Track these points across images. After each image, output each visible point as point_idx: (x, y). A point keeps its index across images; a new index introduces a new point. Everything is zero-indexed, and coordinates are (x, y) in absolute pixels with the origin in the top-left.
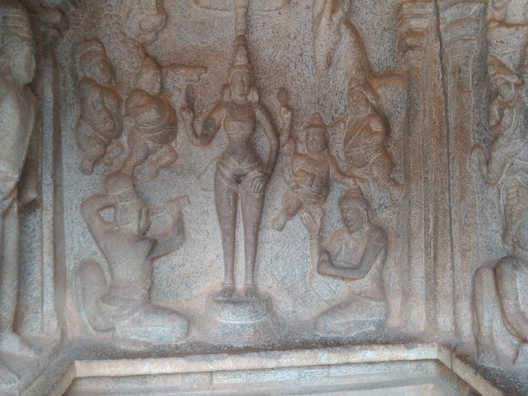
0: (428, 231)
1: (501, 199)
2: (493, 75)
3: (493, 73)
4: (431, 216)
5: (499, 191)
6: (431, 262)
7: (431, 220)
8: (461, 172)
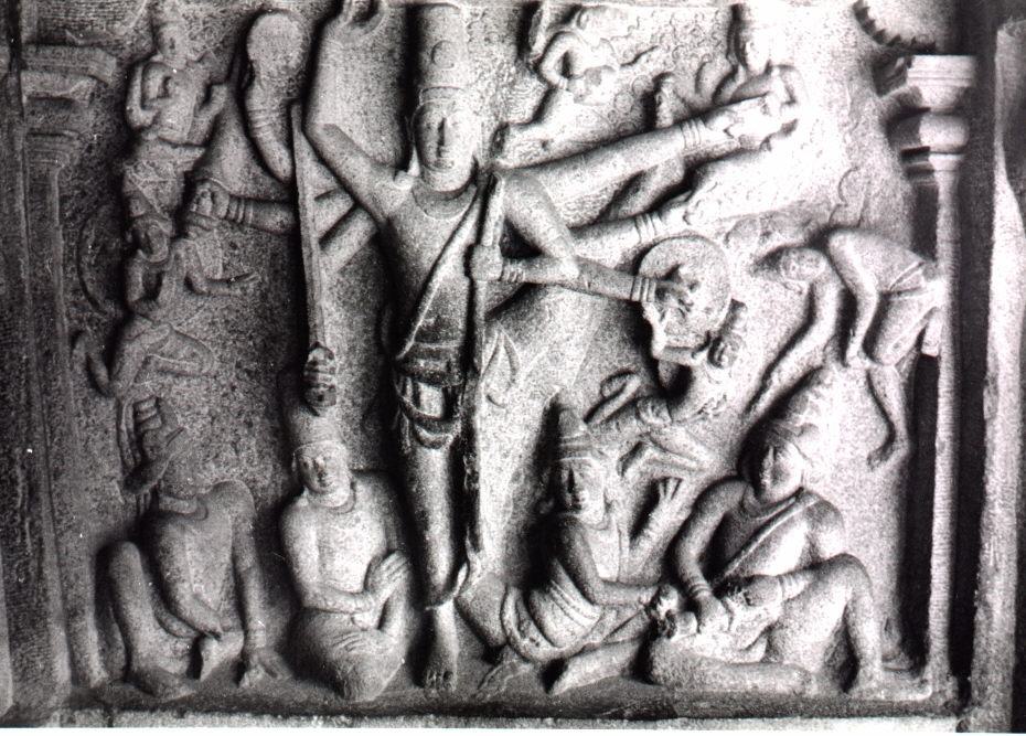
0: (14, 503)
1: (123, 421)
2: (141, 217)
3: (142, 213)
4: (18, 471)
5: (119, 407)
6: (27, 563)
7: (20, 480)
8: (64, 381)
